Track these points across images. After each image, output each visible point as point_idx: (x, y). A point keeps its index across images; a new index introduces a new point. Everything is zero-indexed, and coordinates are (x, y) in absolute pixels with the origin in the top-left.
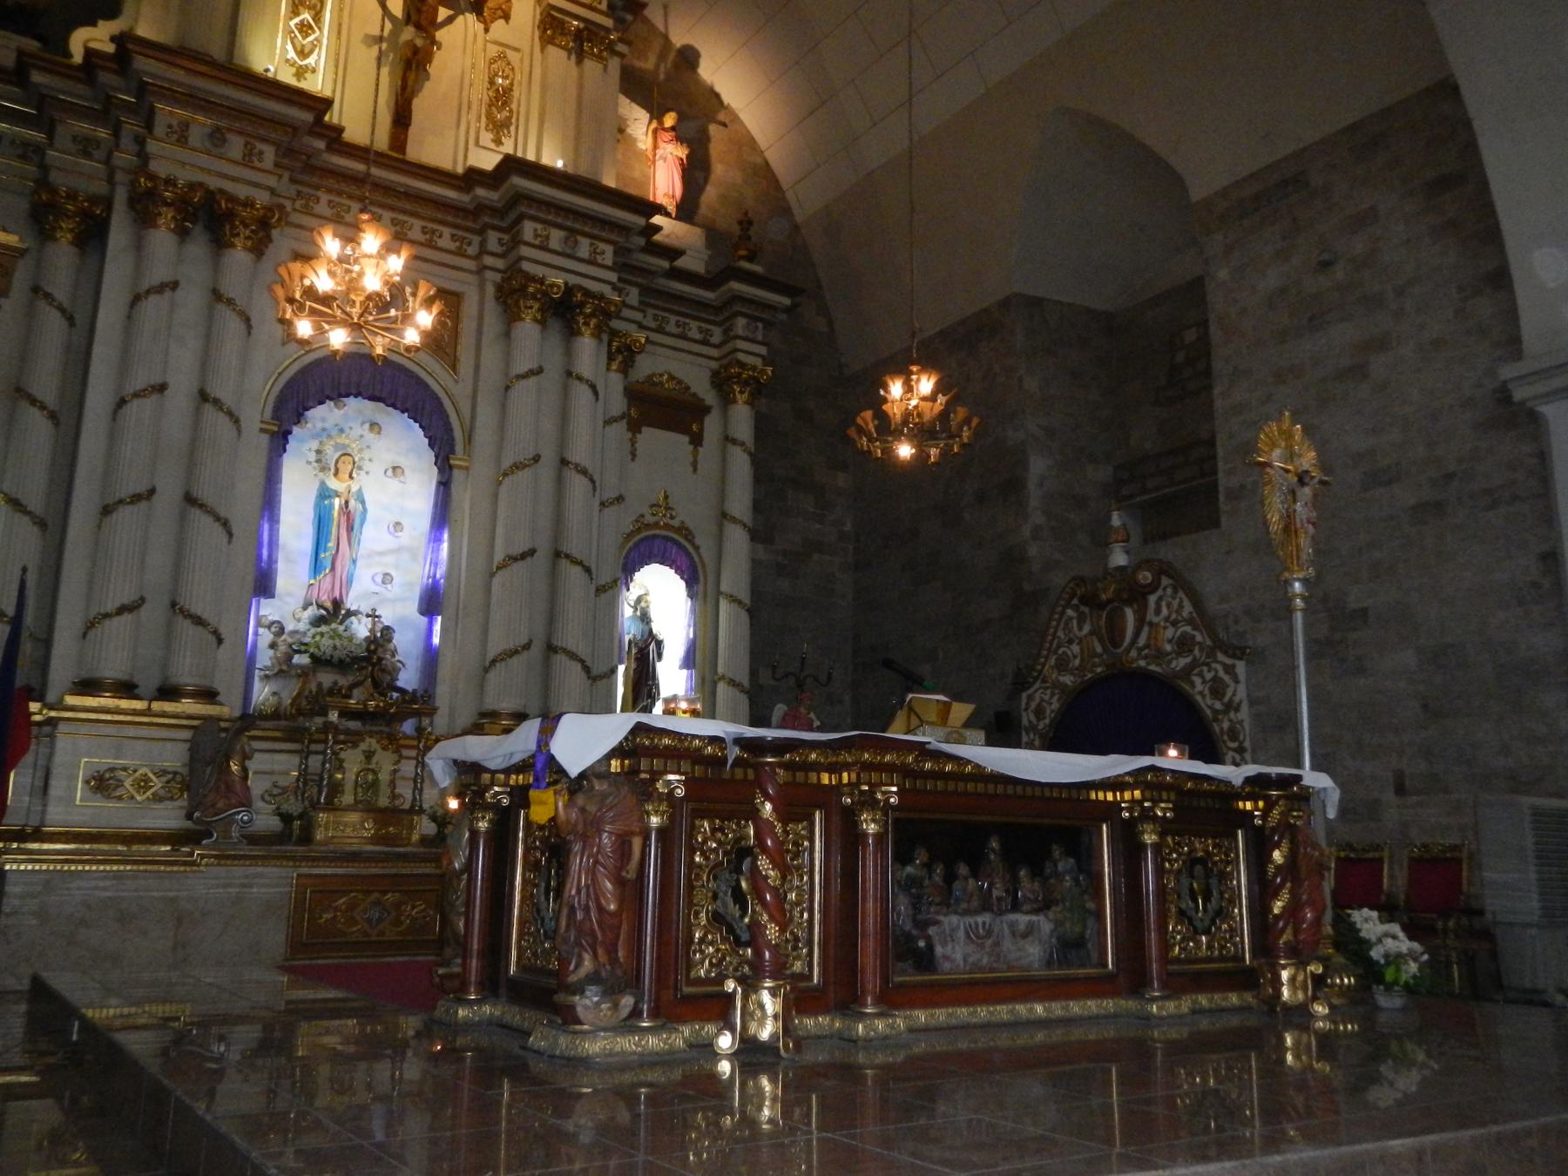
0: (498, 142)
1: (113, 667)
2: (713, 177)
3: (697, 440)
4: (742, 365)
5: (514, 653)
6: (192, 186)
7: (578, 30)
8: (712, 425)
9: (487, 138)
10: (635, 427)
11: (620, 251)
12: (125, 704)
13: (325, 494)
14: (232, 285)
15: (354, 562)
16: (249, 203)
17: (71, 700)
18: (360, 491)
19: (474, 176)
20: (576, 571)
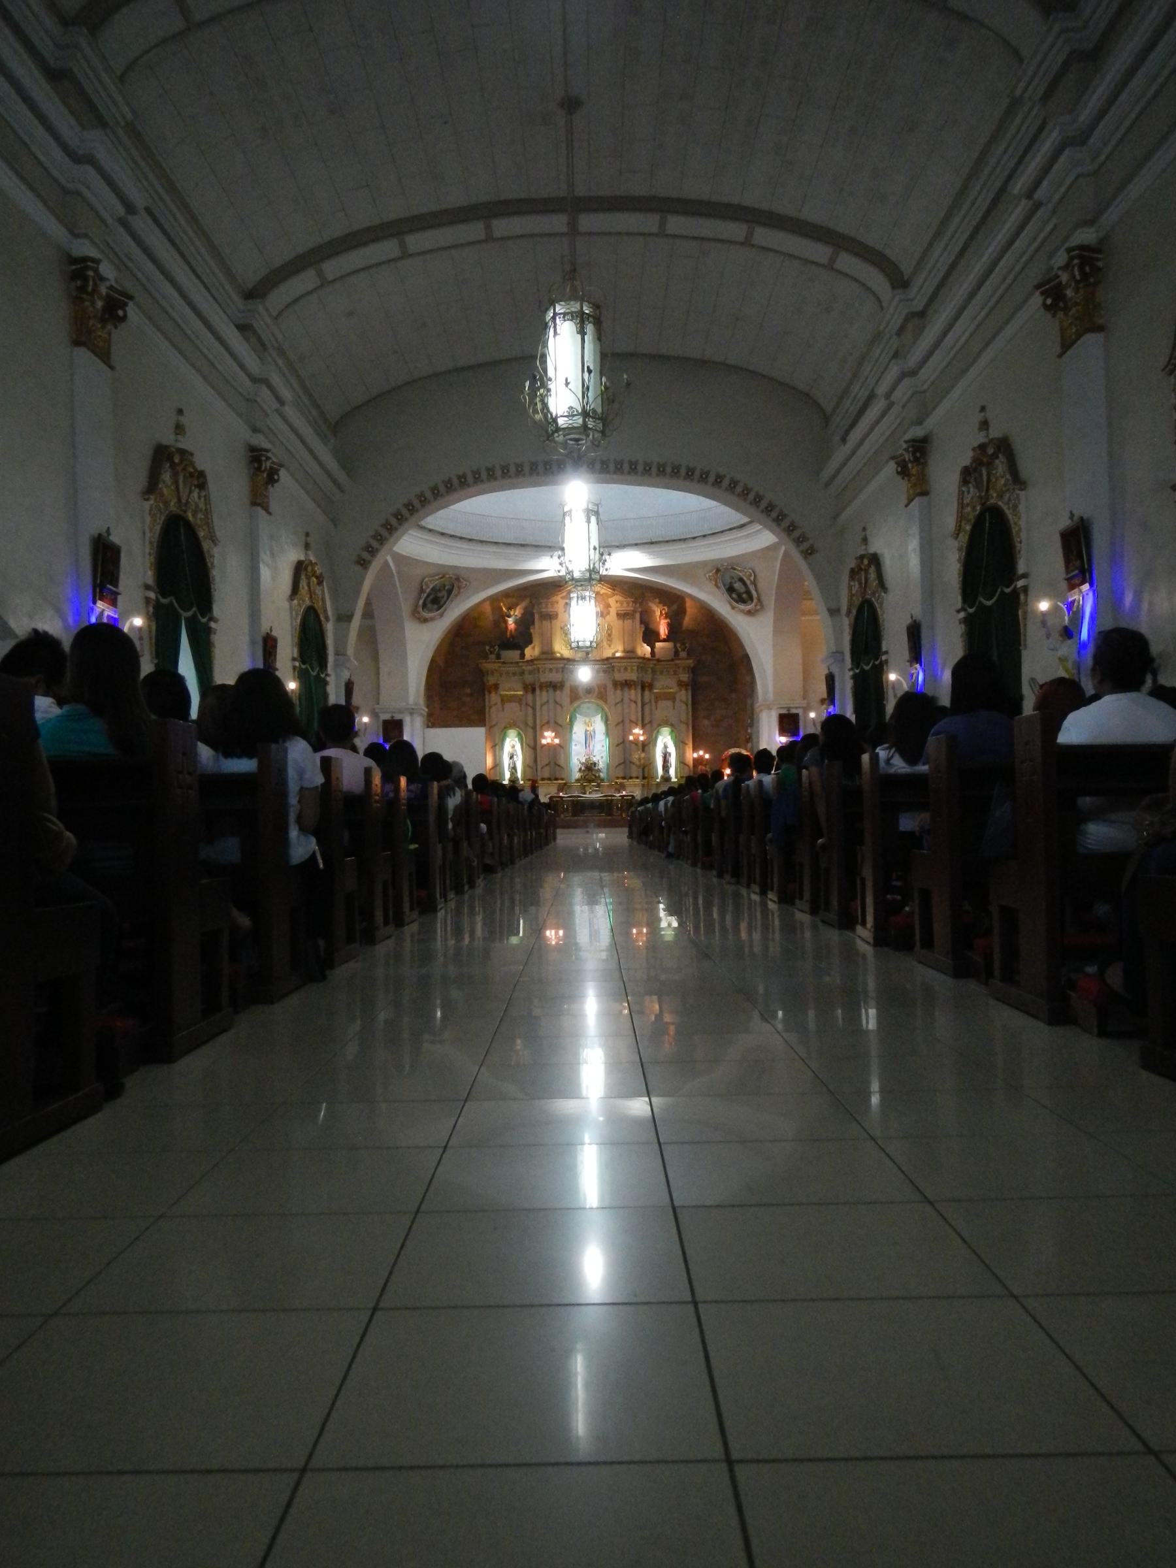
0: (610, 646)
1: (546, 775)
2: (688, 613)
3: (674, 702)
4: (682, 682)
5: (620, 764)
6: (547, 682)
7: (625, 613)
8: (678, 697)
9: (607, 646)
10: (656, 702)
11: (638, 667)
12: (549, 782)
13: (586, 731)
14: (558, 701)
15: (594, 746)
16: (558, 682)
17: (541, 782)
18: (594, 729)
19: (603, 660)
20: (633, 745)
